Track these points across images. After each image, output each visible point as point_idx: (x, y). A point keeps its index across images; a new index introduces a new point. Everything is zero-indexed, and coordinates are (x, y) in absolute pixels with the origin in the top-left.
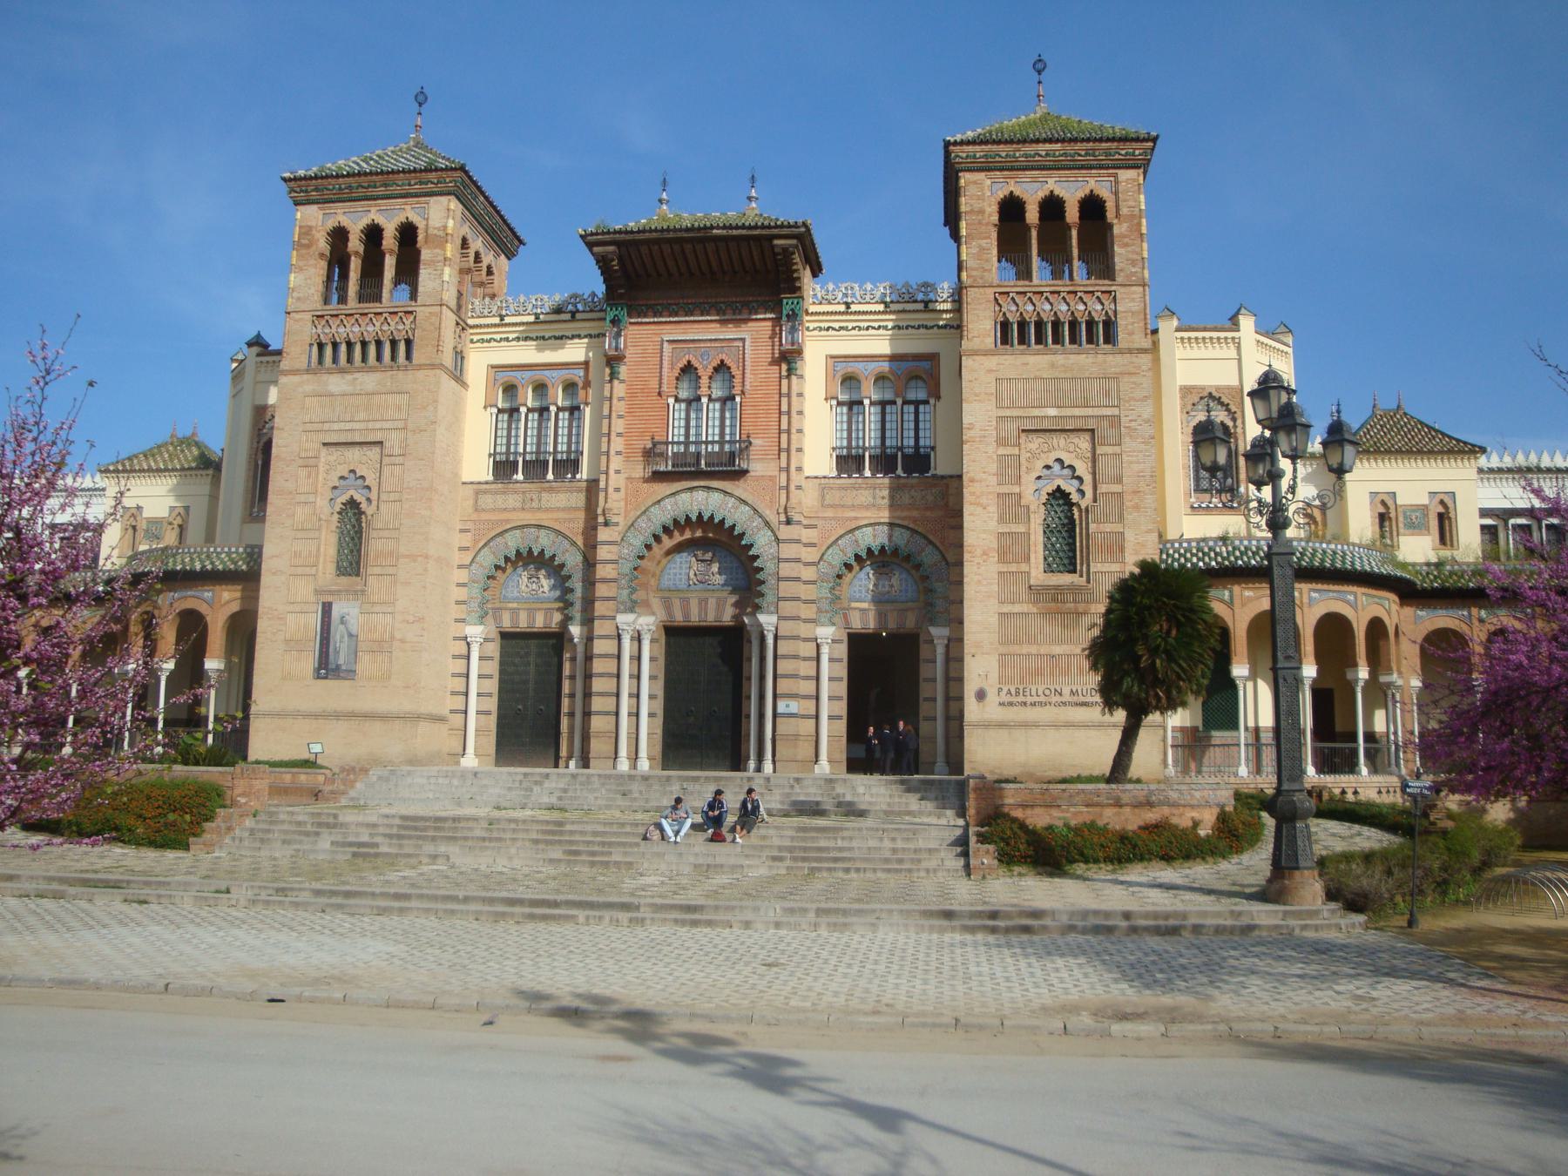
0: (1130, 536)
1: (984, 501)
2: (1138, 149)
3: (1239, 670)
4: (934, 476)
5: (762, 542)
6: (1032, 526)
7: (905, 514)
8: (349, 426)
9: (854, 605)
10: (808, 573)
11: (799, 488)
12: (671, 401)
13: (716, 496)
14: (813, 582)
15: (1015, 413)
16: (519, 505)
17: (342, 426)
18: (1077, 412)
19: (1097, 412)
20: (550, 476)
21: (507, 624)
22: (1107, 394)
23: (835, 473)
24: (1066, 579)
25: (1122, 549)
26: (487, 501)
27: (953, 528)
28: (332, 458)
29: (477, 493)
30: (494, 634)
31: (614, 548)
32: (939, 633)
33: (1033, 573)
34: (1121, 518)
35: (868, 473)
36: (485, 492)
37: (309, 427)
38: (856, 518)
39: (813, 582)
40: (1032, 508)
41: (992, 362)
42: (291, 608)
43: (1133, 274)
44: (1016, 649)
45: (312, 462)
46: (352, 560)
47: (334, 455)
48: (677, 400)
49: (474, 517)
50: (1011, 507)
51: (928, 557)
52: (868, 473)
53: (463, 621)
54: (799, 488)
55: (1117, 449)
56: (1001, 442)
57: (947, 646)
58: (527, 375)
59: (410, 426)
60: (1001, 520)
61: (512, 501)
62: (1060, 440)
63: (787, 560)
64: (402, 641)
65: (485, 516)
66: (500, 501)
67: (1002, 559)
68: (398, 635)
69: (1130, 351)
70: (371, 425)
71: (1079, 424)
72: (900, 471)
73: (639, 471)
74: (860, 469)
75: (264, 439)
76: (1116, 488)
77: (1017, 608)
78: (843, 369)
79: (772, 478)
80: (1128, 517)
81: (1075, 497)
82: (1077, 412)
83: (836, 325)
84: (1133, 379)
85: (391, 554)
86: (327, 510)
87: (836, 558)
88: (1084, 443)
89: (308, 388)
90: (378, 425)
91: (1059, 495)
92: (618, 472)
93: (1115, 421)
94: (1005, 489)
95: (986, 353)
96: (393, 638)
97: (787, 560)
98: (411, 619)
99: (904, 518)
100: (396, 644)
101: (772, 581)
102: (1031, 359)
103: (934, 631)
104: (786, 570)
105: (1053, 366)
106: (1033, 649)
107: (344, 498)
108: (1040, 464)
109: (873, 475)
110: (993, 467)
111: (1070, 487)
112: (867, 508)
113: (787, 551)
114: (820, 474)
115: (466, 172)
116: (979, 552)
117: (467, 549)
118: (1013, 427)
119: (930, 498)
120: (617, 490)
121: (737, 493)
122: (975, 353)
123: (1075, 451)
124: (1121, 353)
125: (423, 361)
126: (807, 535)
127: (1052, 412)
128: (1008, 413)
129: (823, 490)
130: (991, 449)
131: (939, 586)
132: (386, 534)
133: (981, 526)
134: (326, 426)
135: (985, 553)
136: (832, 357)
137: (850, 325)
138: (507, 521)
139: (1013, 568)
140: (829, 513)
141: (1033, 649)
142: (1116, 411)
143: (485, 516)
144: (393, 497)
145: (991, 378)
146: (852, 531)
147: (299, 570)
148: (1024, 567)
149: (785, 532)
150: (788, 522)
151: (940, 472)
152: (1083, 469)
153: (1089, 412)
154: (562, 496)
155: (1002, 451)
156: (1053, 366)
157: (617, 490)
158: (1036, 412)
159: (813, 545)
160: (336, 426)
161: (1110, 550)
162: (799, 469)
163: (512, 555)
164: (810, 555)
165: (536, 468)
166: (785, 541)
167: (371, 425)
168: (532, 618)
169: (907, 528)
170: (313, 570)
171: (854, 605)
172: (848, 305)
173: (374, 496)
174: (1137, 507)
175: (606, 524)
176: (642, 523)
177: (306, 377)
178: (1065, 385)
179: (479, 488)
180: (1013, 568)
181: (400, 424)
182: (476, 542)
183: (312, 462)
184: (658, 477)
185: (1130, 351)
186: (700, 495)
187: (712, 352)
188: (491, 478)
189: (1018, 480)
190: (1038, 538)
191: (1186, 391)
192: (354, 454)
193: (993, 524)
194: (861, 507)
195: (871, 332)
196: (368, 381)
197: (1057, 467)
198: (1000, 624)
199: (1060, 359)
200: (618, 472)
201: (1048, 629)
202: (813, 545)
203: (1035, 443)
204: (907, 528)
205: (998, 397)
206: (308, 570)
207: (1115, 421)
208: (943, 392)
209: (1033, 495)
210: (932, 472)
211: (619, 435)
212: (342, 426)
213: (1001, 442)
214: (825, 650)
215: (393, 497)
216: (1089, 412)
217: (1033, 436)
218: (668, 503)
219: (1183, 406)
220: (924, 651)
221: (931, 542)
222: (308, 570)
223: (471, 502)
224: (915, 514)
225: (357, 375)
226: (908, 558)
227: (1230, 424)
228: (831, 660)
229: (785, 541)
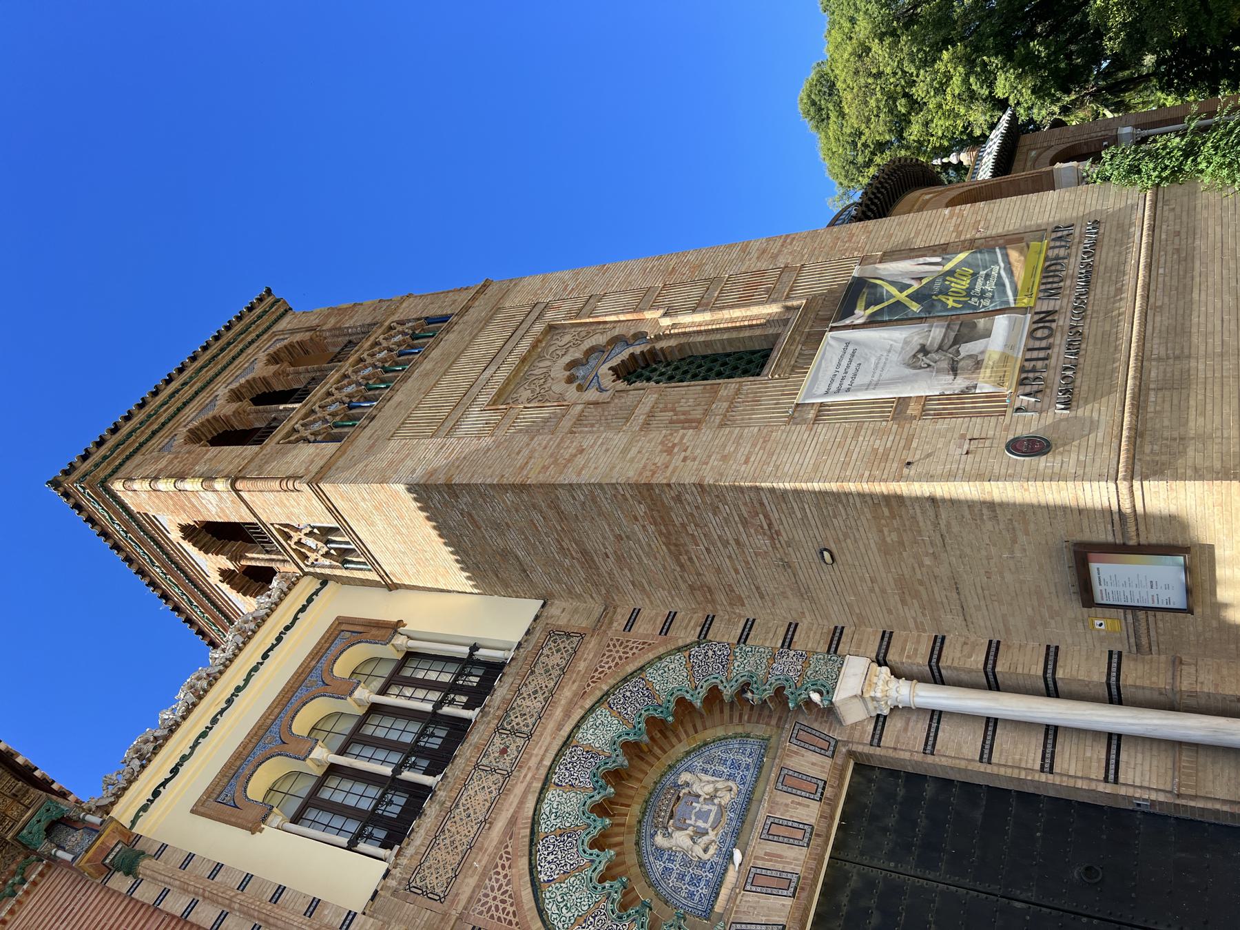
7: (558, 713)
27: (629, 626)
32: (860, 687)
38: (513, 821)
51: (671, 679)
57: (897, 674)
99: (567, 714)
102: (398, 398)
111: (621, 355)
112: (503, 791)
116: (660, 460)
119: (556, 659)
129: (411, 889)
131: (741, 667)
135: (669, 451)
140: (468, 884)
156: (427, 375)
169: (592, 709)
194: (494, 806)
204: (592, 709)
221: (642, 669)
226: (656, 726)
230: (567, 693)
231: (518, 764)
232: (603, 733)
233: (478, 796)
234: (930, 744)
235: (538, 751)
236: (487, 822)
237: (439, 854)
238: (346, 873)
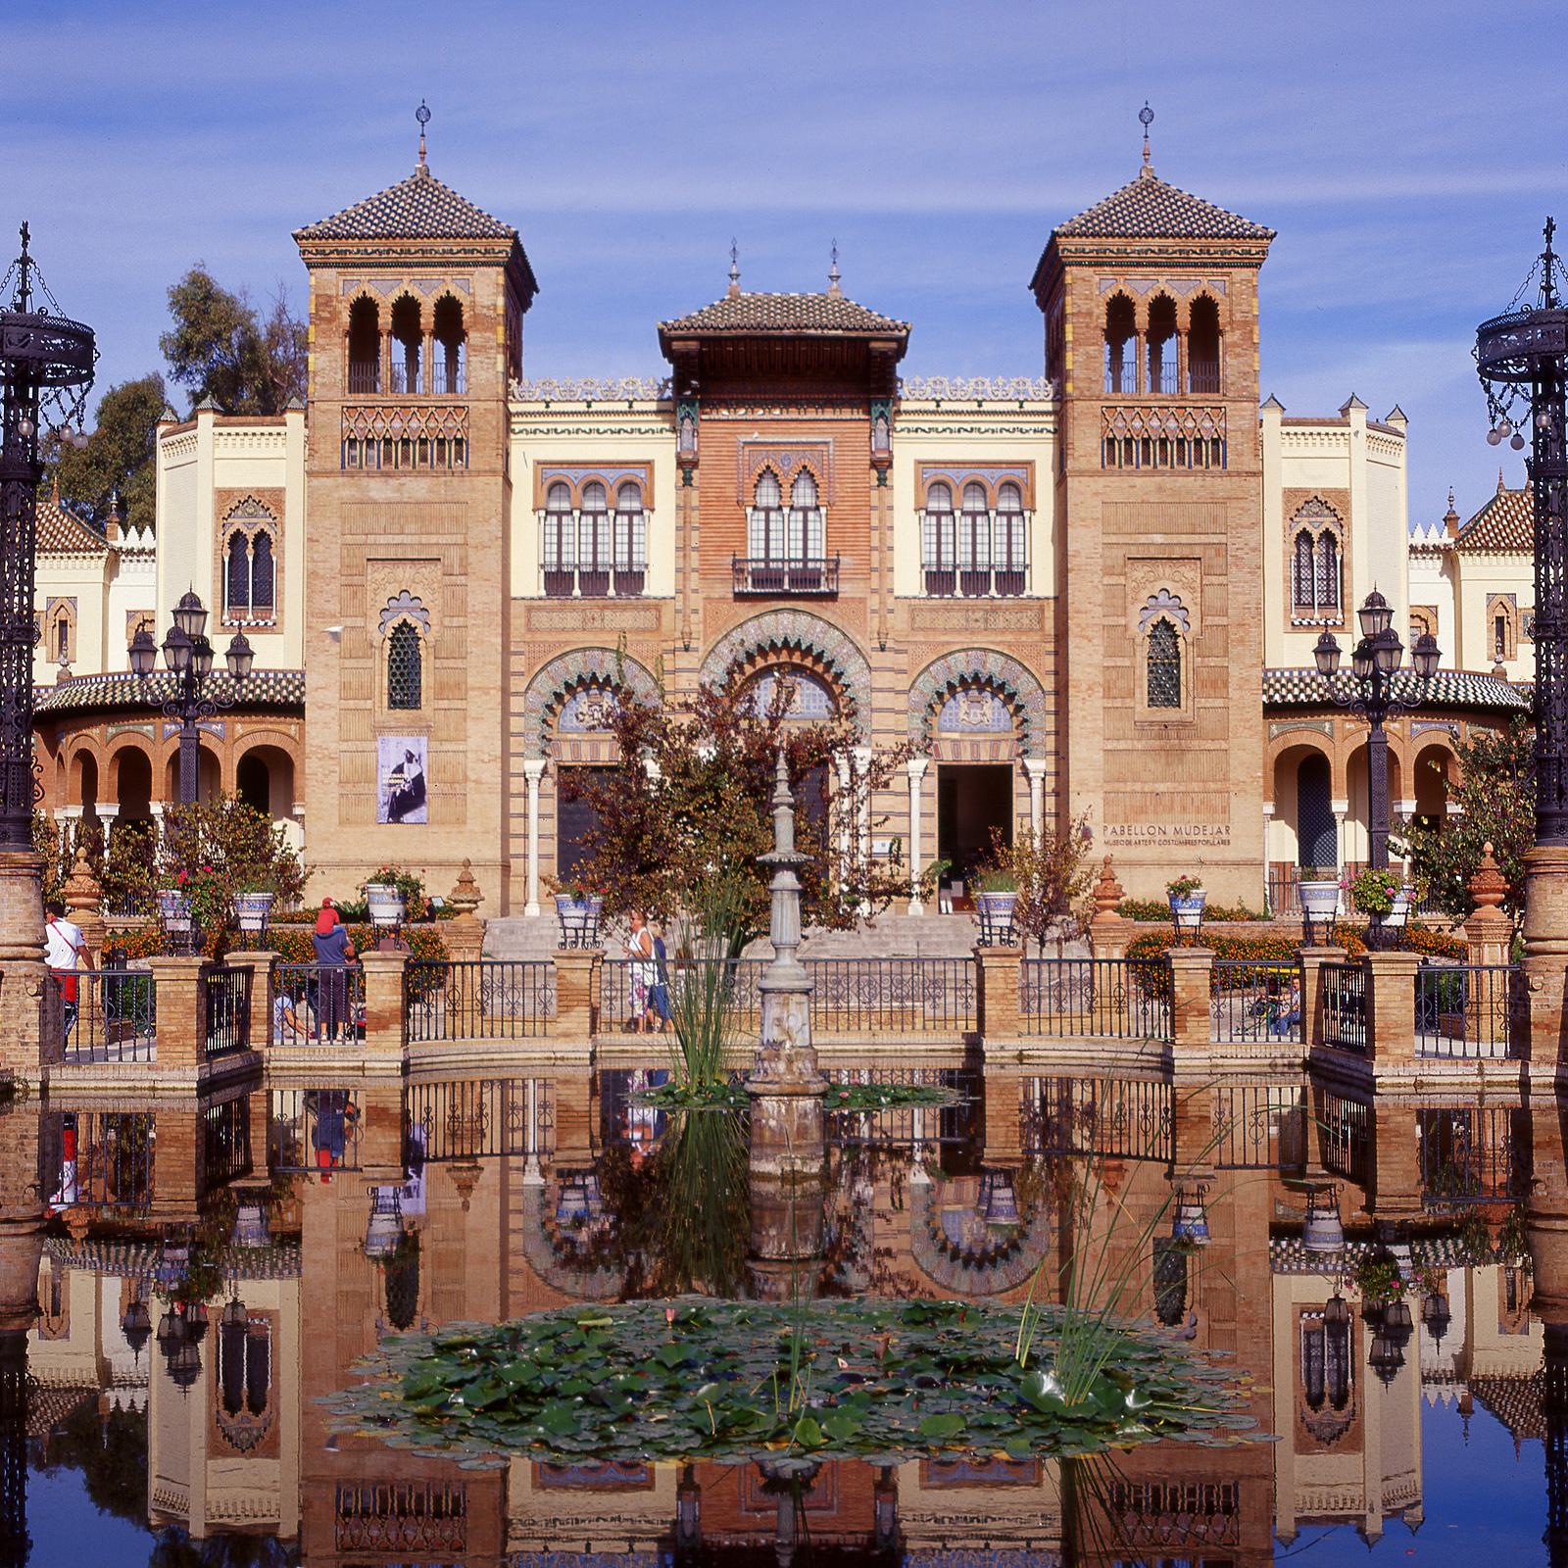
0: (1235, 672)
1: (1089, 633)
2: (1253, 246)
3: (1339, 805)
4: (1030, 598)
5: (853, 671)
6: (1139, 658)
8: (398, 539)
9: (944, 735)
10: (901, 702)
11: (891, 611)
12: (749, 510)
13: (804, 619)
14: (905, 712)
15: (1122, 539)
16: (578, 624)
17: (390, 539)
18: (1184, 539)
19: (1204, 539)
20: (611, 592)
21: (567, 757)
22: (1215, 520)
23: (925, 594)
24: (1170, 714)
25: (1226, 685)
26: (542, 619)
28: (378, 576)
29: (529, 609)
30: (553, 770)
31: (694, 676)
33: (1139, 708)
34: (1226, 653)
35: (958, 593)
36: (540, 609)
37: (349, 539)
39: (905, 712)
40: (1138, 640)
41: (1099, 483)
42: (344, 746)
43: (1245, 388)
44: (1121, 786)
45: (357, 580)
46: (405, 689)
47: (377, 574)
48: (755, 508)
49: (528, 637)
50: (1117, 638)
52: (958, 593)
53: (521, 755)
54: (891, 611)
55: (1222, 579)
56: (1108, 571)
58: (582, 472)
59: (471, 541)
60: (1108, 655)
61: (572, 620)
62: (1165, 570)
63: (881, 690)
64: (477, 782)
65: (539, 637)
66: (557, 620)
67: (1107, 695)
68: (472, 776)
69: (1239, 474)
70: (424, 539)
71: (1186, 552)
72: (993, 592)
73: (726, 591)
74: (951, 589)
75: (232, 530)
76: (1224, 621)
77: (1122, 745)
78: (932, 475)
79: (862, 600)
80: (1233, 651)
81: (1179, 629)
82: (1184, 539)
83: (925, 426)
84: (1242, 504)
85: (458, 686)
86: (377, 637)
87: (928, 685)
88: (1190, 572)
89: (346, 493)
90: (433, 539)
91: (1165, 624)
92: (695, 591)
93: (1221, 548)
94: (1111, 621)
95: (1093, 474)
96: (466, 779)
97: (881, 690)
98: (486, 758)
100: (471, 785)
101: (863, 712)
102: (1138, 481)
103: (1029, 763)
104: (879, 700)
105: (1160, 489)
106: (1138, 787)
107: (396, 622)
108: (1145, 594)
109: (966, 595)
110: (1099, 598)
112: (959, 631)
113: (882, 680)
114: (910, 594)
115: (518, 249)
116: (1084, 687)
117: (522, 674)
118: (1120, 553)
119: (1026, 621)
120: (696, 611)
121: (826, 615)
122: (1081, 473)
123: (1180, 581)
124: (1229, 475)
125: (481, 467)
126: (902, 660)
127: (1158, 539)
128: (1114, 539)
129: (913, 610)
130: (1096, 579)
132: (451, 663)
133: (1086, 659)
134: (371, 539)
136: (920, 462)
137: (940, 427)
138: (567, 643)
139: (1118, 703)
141: (1138, 787)
142: (1222, 539)
143: (539, 637)
144: (456, 621)
145: (1097, 502)
146: (944, 657)
147: (351, 704)
148: (1129, 702)
149: (877, 659)
150: (883, 649)
151: (1036, 593)
152: (1187, 600)
153: (1196, 539)
154: (627, 614)
155: (1107, 580)
157: (696, 611)
158: (1143, 539)
159: (904, 672)
160: (382, 539)
161: (1214, 685)
162: (891, 591)
163: (573, 681)
164: (903, 683)
165: (594, 580)
166: (877, 669)
167: (424, 539)
168: (595, 750)
170: (369, 704)
171: (944, 735)
172: (938, 403)
173: (434, 618)
174: (1241, 641)
175: (687, 649)
176: (724, 649)
177: (340, 480)
178: (1172, 510)
179: (531, 606)
180: (1118, 703)
181: (460, 539)
182: (531, 666)
183: (357, 580)
184: (740, 597)
185: (1239, 474)
186: (786, 619)
187: (794, 457)
188: (543, 593)
189: (1125, 615)
190: (1143, 672)
191: (1290, 494)
192: (405, 572)
193: (1098, 658)
195: (964, 434)
196: (418, 487)
197: (1163, 597)
198: (1106, 762)
199: (1168, 482)
200: (695, 591)
201: (1152, 766)
202: (904, 672)
203: (1140, 572)
205: (1105, 521)
206: (362, 704)
207: (1221, 548)
208: (1038, 506)
209: (1138, 625)
210: (1027, 593)
211: (694, 549)
212: (390, 539)
213: (1108, 571)
214: (915, 784)
215: (456, 621)
216: (1196, 539)
217: (1139, 564)
218: (751, 627)
219: (1286, 511)
220: (1018, 784)
221: (1026, 669)
222: (362, 704)
223: (523, 621)
224: (1009, 638)
225: (403, 480)
226: (1002, 687)
227: (1336, 531)
228: (923, 794)
229: (877, 669)
230: (1009, 638)
231: (972, 632)
232: (993, 666)
233: (957, 619)
234: (1020, 795)
235: (980, 638)
236: (945, 631)
237: (928, 615)
238: (908, 580)
